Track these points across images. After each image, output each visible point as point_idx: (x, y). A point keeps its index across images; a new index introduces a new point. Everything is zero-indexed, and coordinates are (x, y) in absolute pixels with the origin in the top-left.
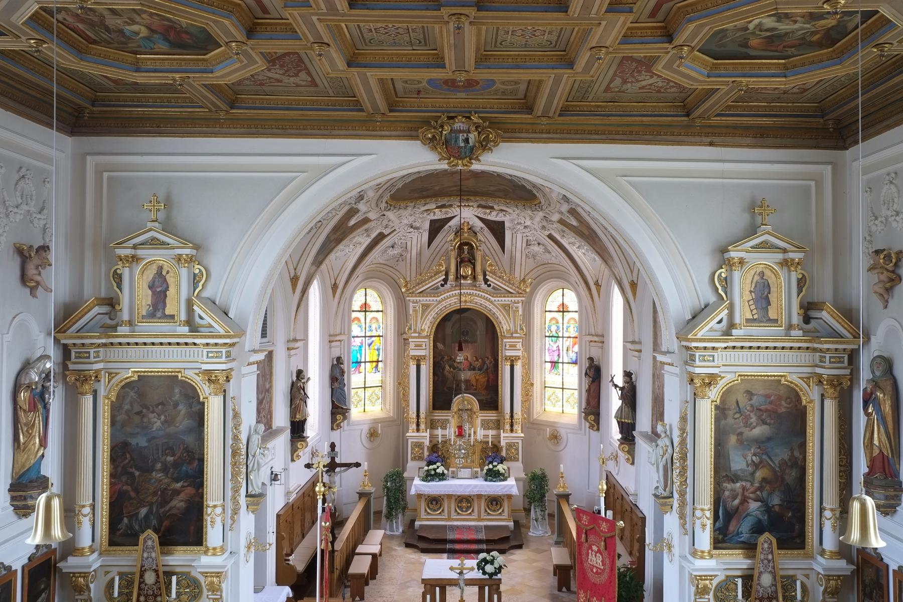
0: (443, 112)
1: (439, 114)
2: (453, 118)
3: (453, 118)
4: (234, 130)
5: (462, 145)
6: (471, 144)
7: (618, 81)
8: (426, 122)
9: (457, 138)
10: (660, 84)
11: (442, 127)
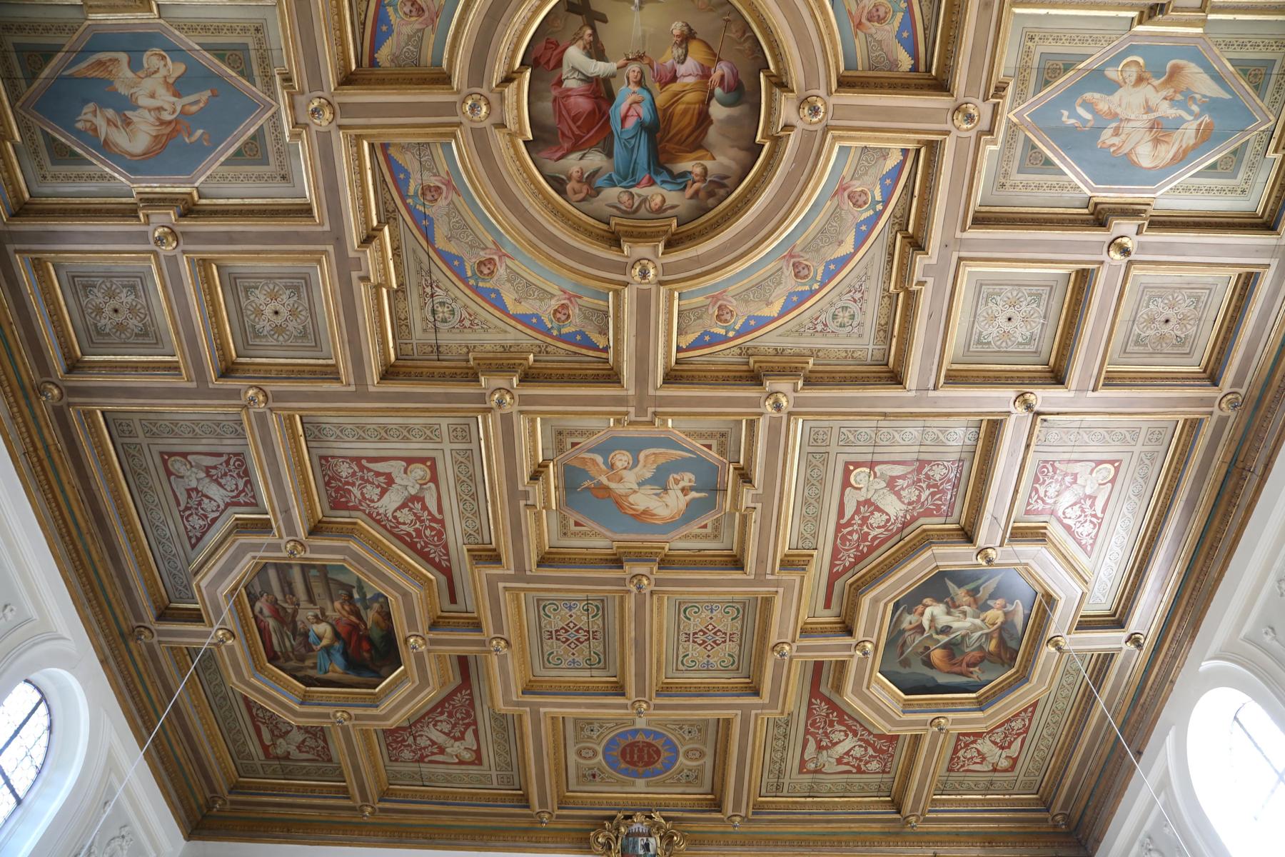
0: (620, 811)
1: (613, 813)
2: (630, 817)
3: (630, 817)
4: (374, 839)
5: (641, 852)
6: (652, 852)
7: (812, 745)
8: (599, 823)
9: (635, 843)
10: (858, 752)
11: (618, 829)
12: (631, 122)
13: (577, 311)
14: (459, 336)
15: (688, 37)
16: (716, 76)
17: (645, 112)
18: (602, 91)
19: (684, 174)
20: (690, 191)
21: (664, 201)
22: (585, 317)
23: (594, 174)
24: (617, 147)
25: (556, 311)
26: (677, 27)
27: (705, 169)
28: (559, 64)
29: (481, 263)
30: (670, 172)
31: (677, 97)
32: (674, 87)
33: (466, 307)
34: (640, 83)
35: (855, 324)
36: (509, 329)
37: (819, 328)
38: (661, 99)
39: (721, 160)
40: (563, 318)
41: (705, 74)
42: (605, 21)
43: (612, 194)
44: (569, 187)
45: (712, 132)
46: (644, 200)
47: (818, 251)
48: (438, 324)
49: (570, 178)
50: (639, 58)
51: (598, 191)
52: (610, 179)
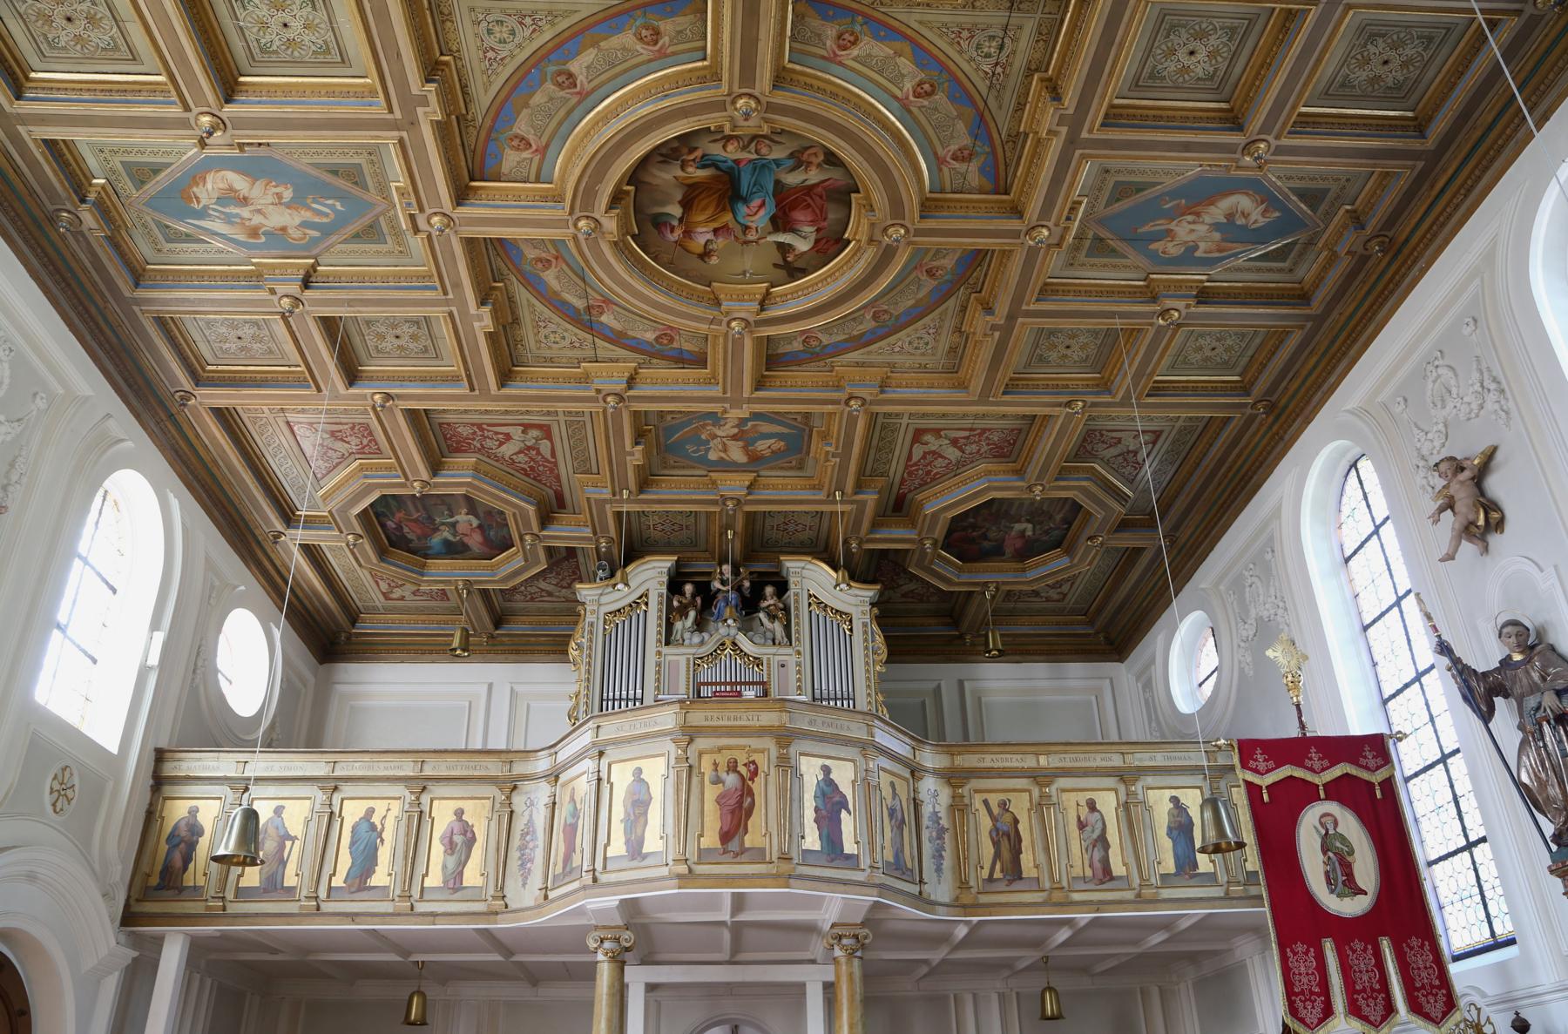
12: (756, 202)
13: (829, 43)
14: (978, 20)
15: (705, 255)
16: (678, 233)
17: (742, 209)
18: (781, 222)
19: (704, 167)
20: (698, 153)
21: (724, 147)
22: (819, 36)
23: (793, 170)
24: (770, 187)
25: (854, 43)
26: (714, 261)
27: (683, 168)
28: (817, 241)
29: (928, 94)
30: (718, 168)
31: (712, 219)
32: (716, 225)
33: (961, 52)
34: (746, 228)
35: (484, 24)
36: (915, 26)
37: (528, 21)
38: (727, 218)
39: (666, 176)
40: (846, 36)
41: (688, 233)
42: (775, 265)
43: (778, 153)
44: (822, 158)
45: (679, 197)
46: (744, 148)
47: (551, 99)
48: (1001, 34)
49: (819, 165)
50: (747, 243)
51: (792, 155)
52: (778, 165)
